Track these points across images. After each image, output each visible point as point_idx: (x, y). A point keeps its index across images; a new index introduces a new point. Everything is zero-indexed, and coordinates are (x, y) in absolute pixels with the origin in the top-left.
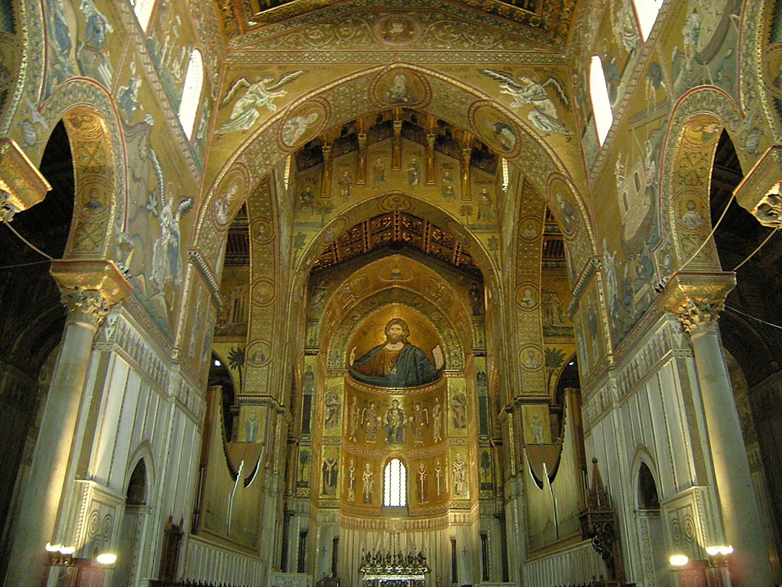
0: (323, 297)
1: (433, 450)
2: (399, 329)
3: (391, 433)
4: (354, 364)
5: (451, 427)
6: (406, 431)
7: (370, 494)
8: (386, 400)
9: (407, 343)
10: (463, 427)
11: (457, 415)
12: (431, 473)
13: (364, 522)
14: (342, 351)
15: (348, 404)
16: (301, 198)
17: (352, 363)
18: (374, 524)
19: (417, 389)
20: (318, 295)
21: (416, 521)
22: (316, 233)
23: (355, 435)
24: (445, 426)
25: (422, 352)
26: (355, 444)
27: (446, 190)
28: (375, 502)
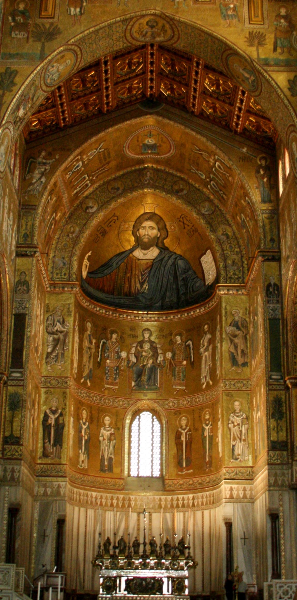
0: (43, 174)
1: (200, 399)
2: (153, 228)
3: (139, 374)
4: (87, 276)
5: (227, 364)
6: (161, 372)
7: (110, 459)
8: (133, 329)
9: (163, 249)
10: (245, 364)
11: (236, 347)
12: (196, 430)
13: (101, 498)
14: (71, 257)
15: (80, 333)
16: (10, 18)
17: (85, 274)
18: (115, 502)
19: (178, 312)
20: (37, 172)
21: (175, 497)
22: (32, 68)
23: (90, 376)
24: (218, 364)
25: (187, 262)
26: (89, 388)
27: (227, 10)
28: (116, 470)
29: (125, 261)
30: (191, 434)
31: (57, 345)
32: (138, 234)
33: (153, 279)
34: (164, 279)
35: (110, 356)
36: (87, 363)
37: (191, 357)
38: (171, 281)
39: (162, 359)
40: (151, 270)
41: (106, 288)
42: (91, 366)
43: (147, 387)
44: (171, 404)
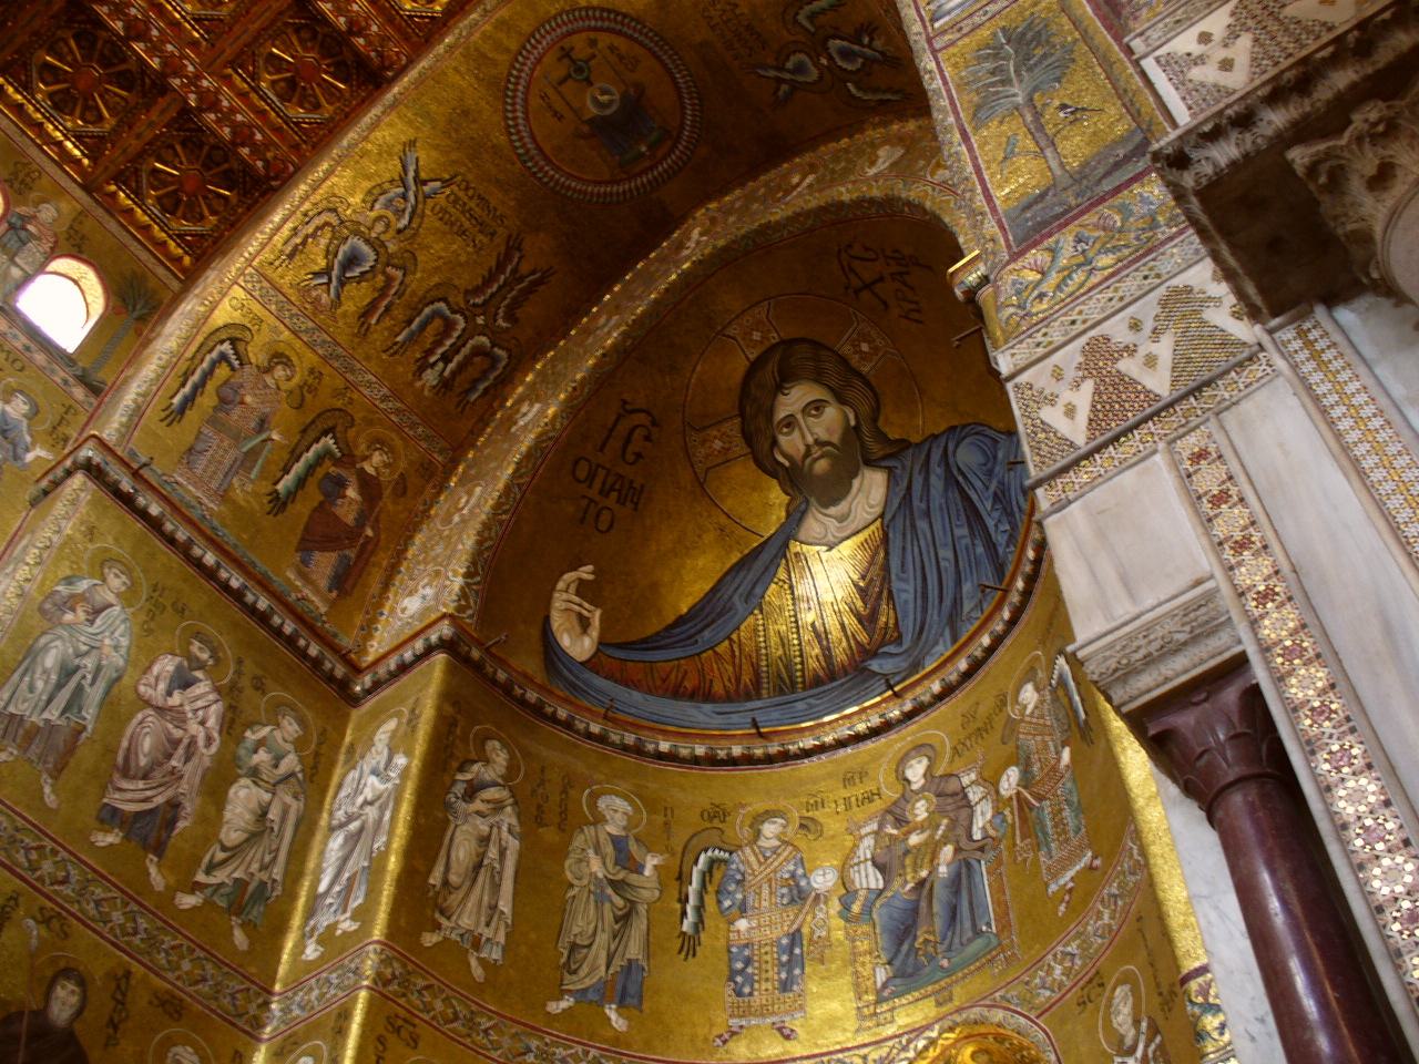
2: (817, 407)
29: (782, 574)
30: (1160, 1047)
31: (352, 851)
32: (780, 459)
33: (905, 581)
34: (942, 553)
35: (750, 901)
36: (603, 938)
37: (1075, 712)
38: (964, 542)
39: (989, 816)
40: (887, 553)
41: (718, 688)
42: (634, 950)
43: (945, 963)
44: (1058, 970)
